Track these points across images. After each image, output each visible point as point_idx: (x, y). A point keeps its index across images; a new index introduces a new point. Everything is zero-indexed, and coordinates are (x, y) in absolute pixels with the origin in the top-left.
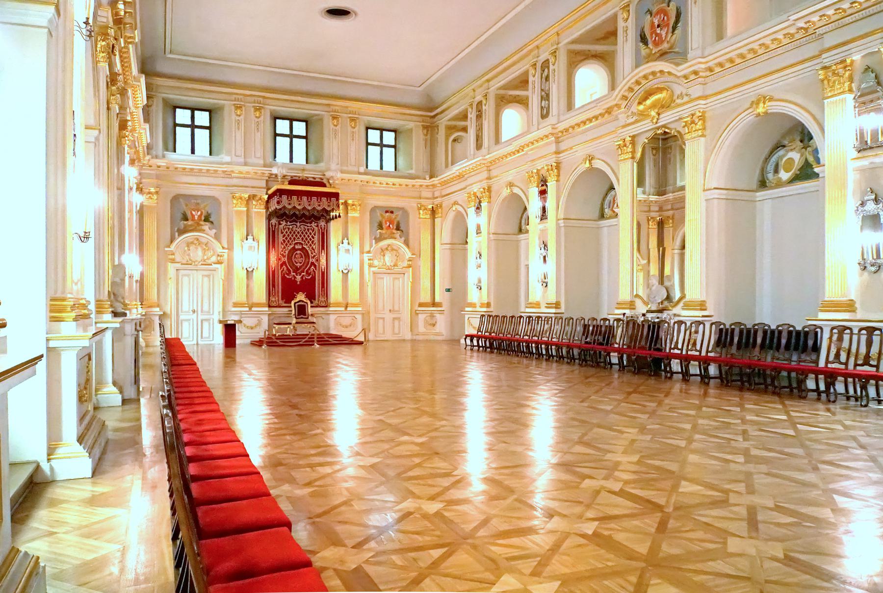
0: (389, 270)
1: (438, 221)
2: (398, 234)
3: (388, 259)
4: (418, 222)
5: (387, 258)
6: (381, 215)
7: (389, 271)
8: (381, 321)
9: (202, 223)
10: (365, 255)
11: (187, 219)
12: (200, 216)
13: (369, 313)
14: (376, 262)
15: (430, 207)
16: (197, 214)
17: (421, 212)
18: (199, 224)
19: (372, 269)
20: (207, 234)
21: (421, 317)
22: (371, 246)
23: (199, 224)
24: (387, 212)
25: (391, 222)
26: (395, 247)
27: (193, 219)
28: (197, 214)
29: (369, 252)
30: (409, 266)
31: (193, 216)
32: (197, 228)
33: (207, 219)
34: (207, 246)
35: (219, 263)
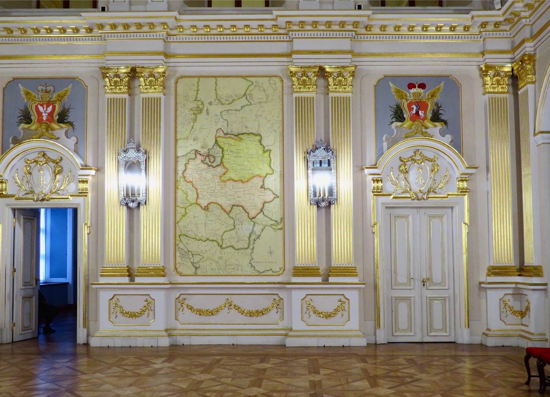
0: (421, 201)
1: (528, 89)
2: (435, 129)
3: (417, 179)
4: (477, 100)
5: (413, 175)
6: (398, 91)
7: (416, 203)
8: (403, 307)
9: (55, 126)
10: (366, 171)
11: (27, 118)
12: (51, 114)
13: (376, 287)
14: (389, 187)
15: (507, 68)
16: (45, 111)
17: (488, 79)
18: (48, 128)
19: (382, 199)
20: (61, 146)
21: (494, 298)
22: (380, 153)
23: (48, 128)
24: (411, 86)
25: (421, 105)
26: (430, 155)
27: (40, 121)
28: (45, 111)
29: (375, 167)
30: (463, 191)
31: (39, 114)
32: (46, 132)
33: (62, 118)
34: (57, 166)
35: (83, 193)
